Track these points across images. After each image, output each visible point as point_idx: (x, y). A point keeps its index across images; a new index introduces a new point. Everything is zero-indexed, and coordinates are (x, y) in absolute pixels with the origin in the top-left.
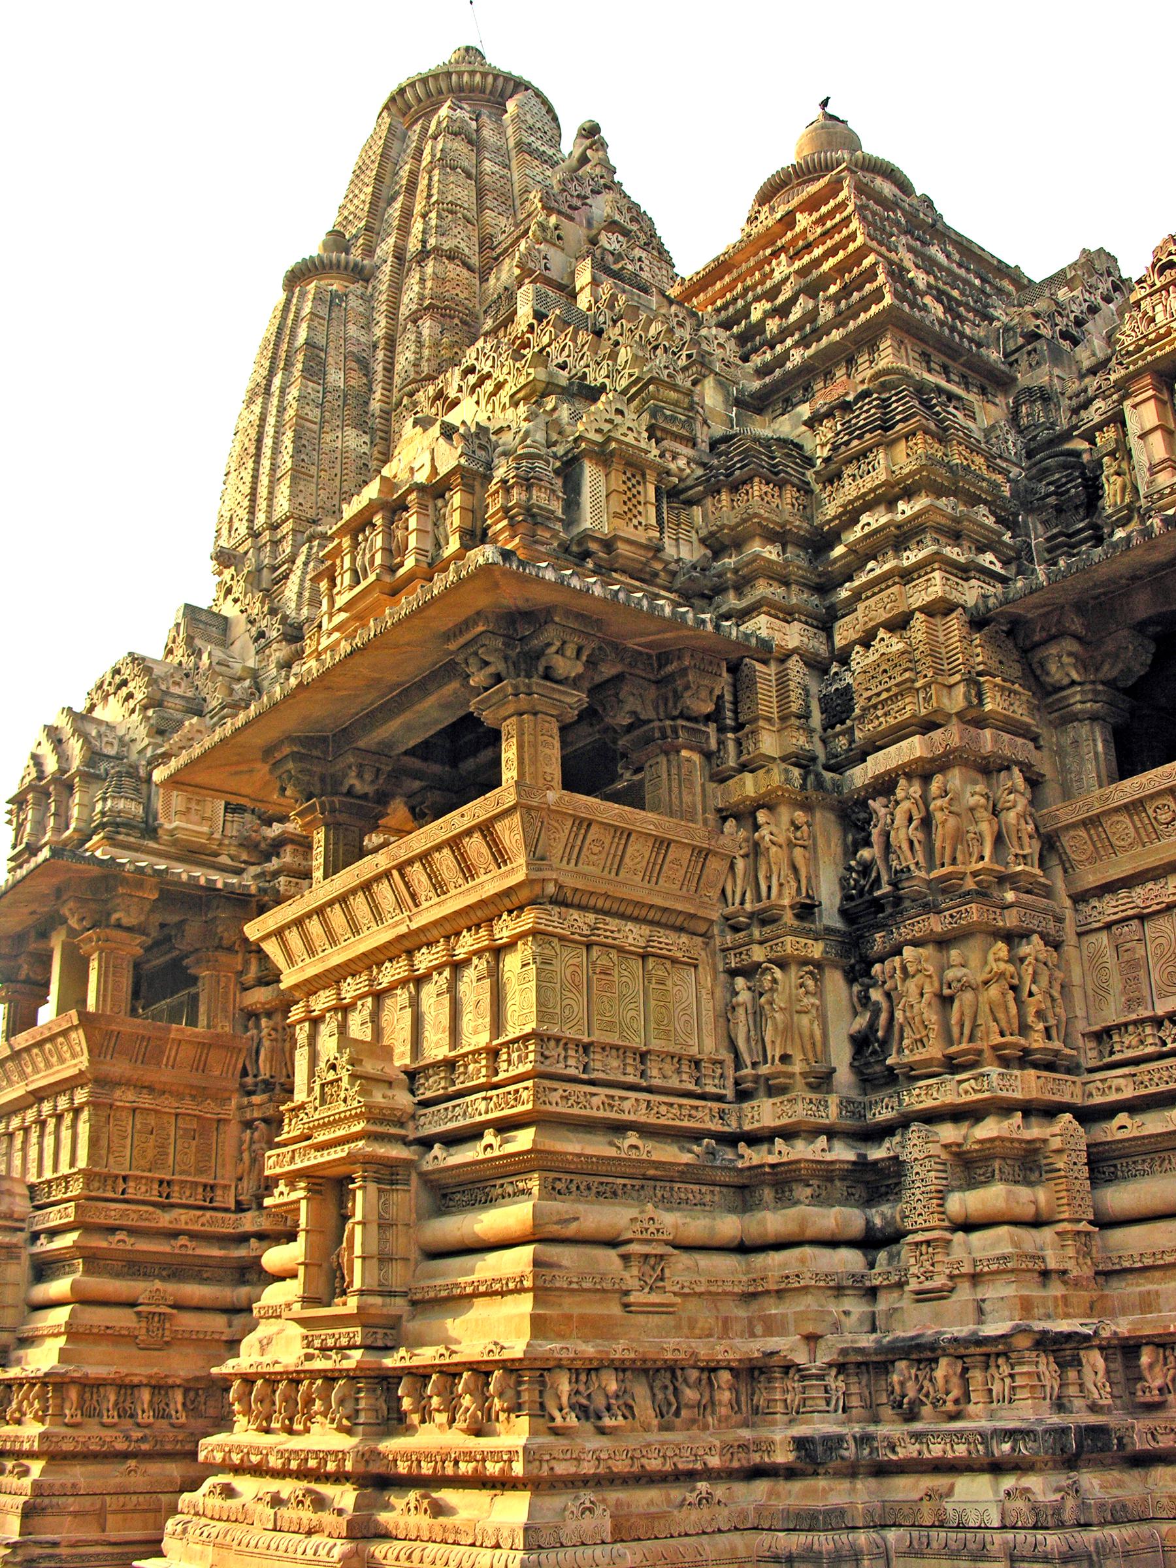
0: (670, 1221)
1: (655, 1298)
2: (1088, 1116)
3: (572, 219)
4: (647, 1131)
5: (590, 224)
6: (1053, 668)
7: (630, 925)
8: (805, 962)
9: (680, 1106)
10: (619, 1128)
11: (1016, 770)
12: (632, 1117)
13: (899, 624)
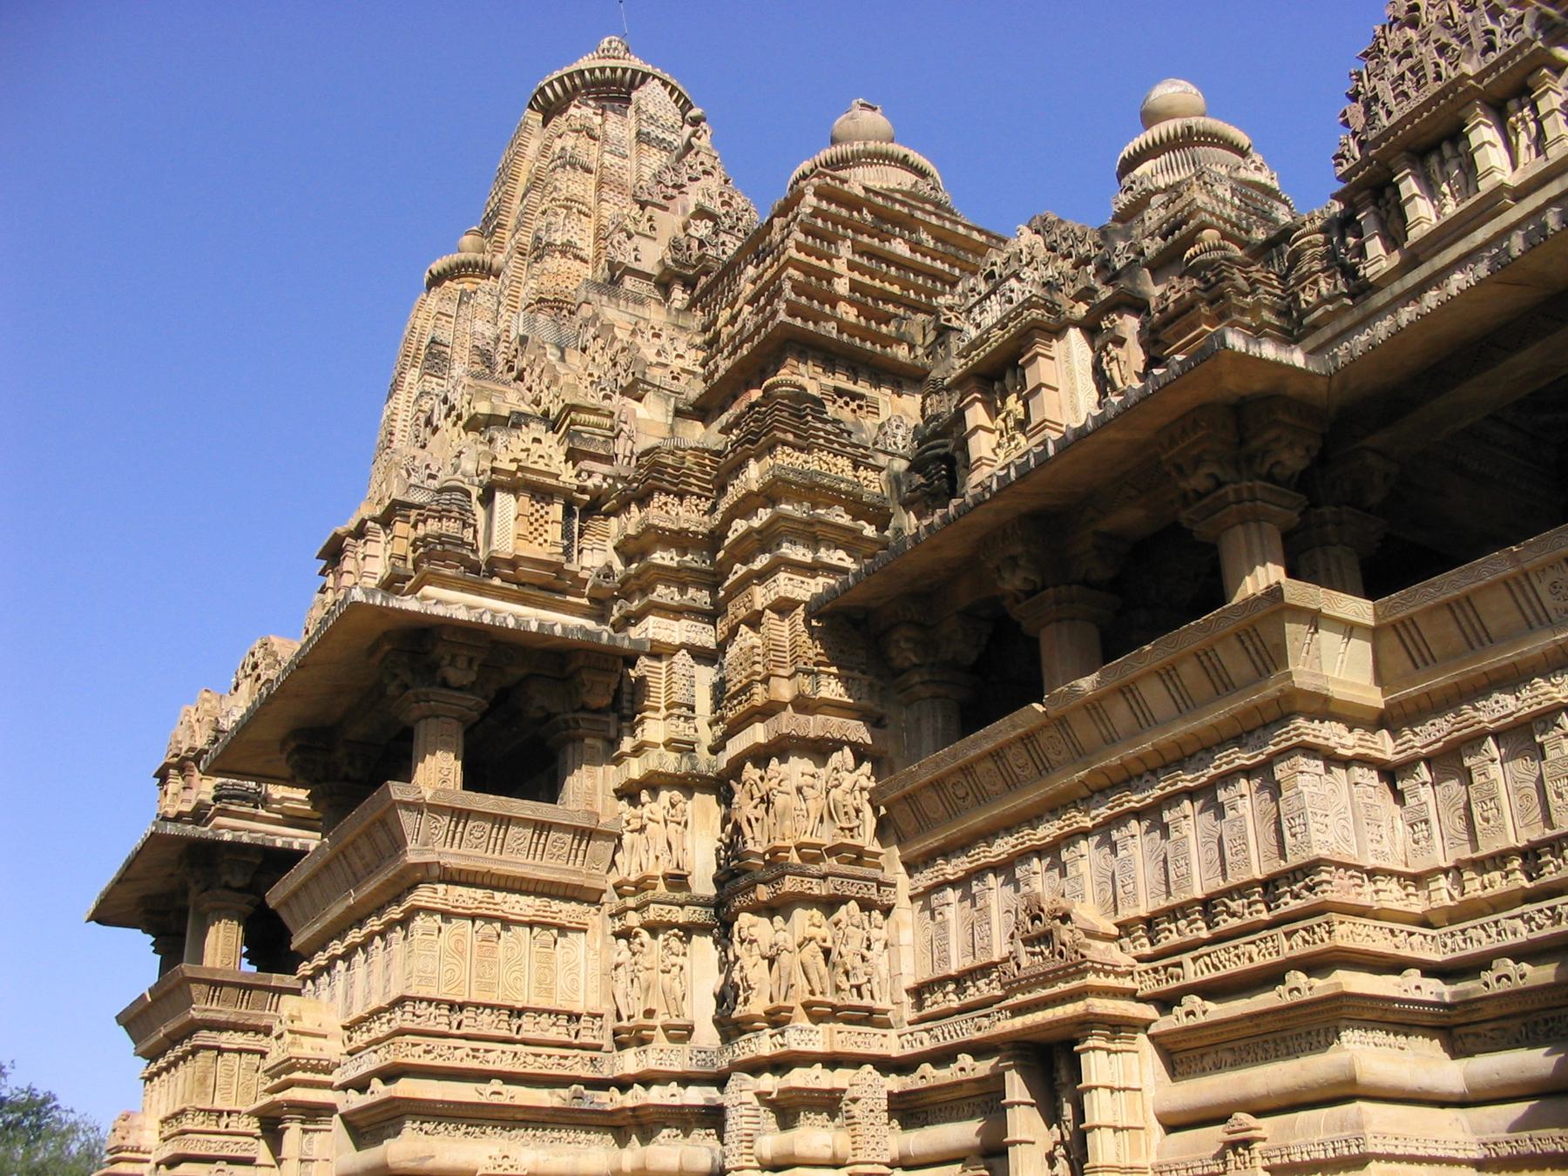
2: (886, 1065)
3: (666, 209)
5: (684, 210)
6: (894, 653)
7: (517, 897)
8: (670, 925)
9: (549, 1056)
10: (484, 1077)
11: (847, 750)
13: (754, 621)
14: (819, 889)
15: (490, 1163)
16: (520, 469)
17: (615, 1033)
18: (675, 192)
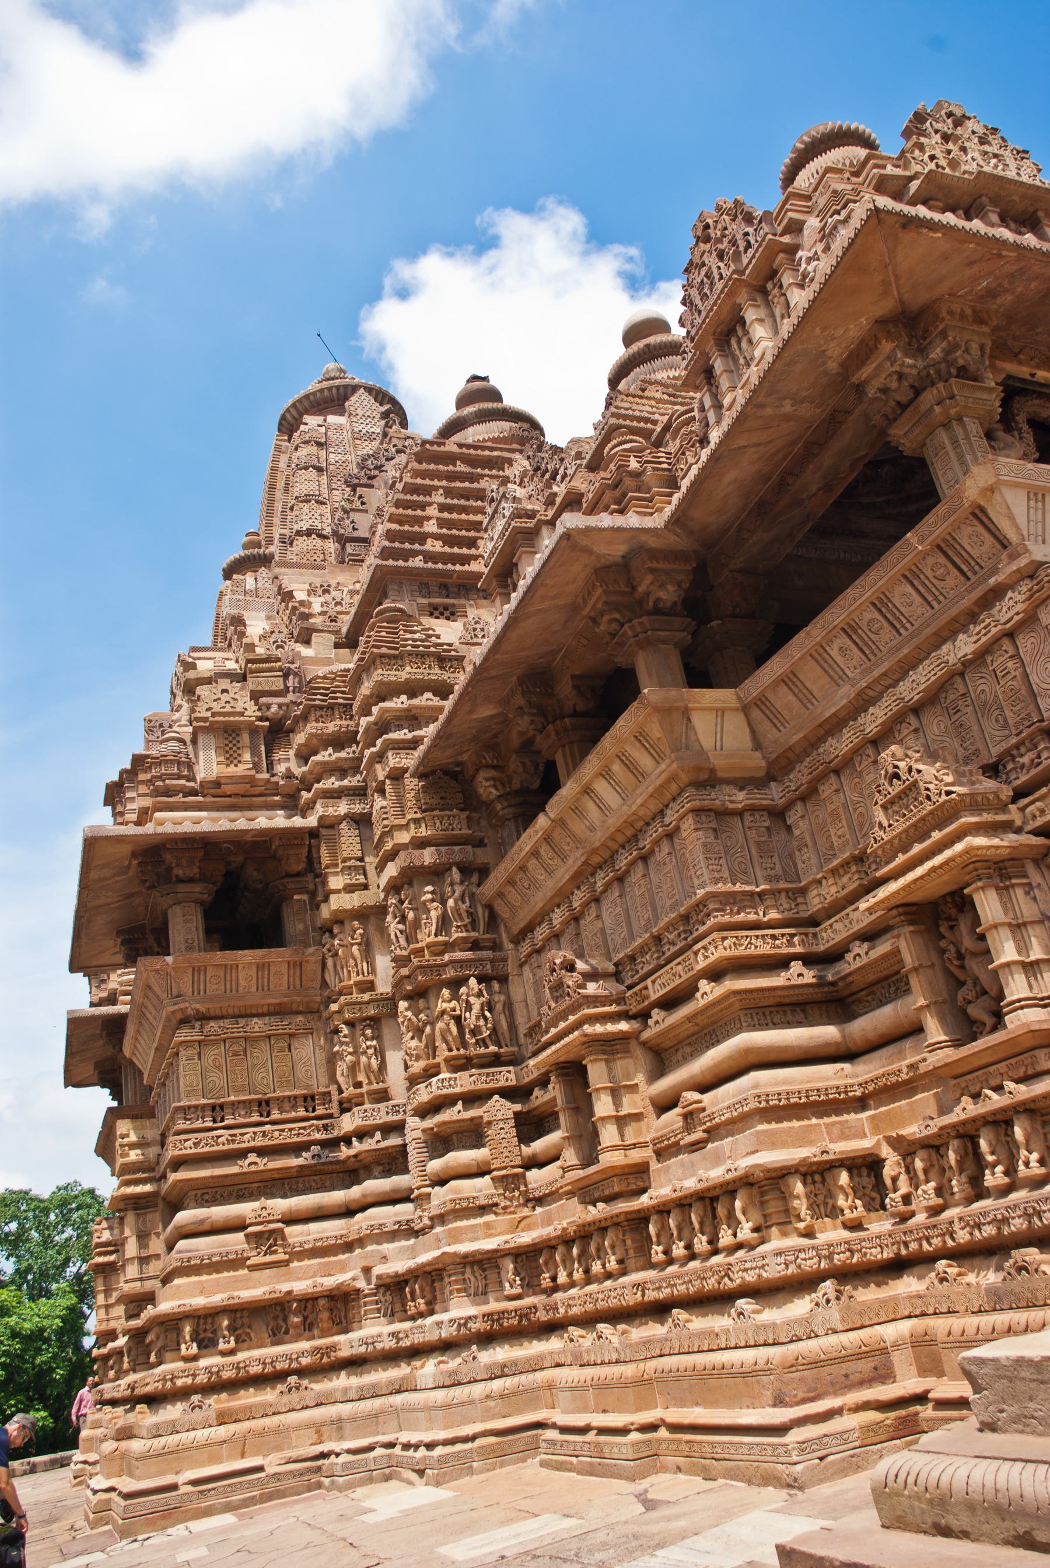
0: (281, 1205)
1: (269, 1258)
3: (372, 486)
4: (261, 1152)
5: (386, 483)
7: (256, 1020)
9: (291, 1130)
11: (454, 869)
12: (252, 1144)
14: (450, 973)
15: (252, 1215)
16: (214, 715)
17: (341, 1103)
18: (377, 472)
